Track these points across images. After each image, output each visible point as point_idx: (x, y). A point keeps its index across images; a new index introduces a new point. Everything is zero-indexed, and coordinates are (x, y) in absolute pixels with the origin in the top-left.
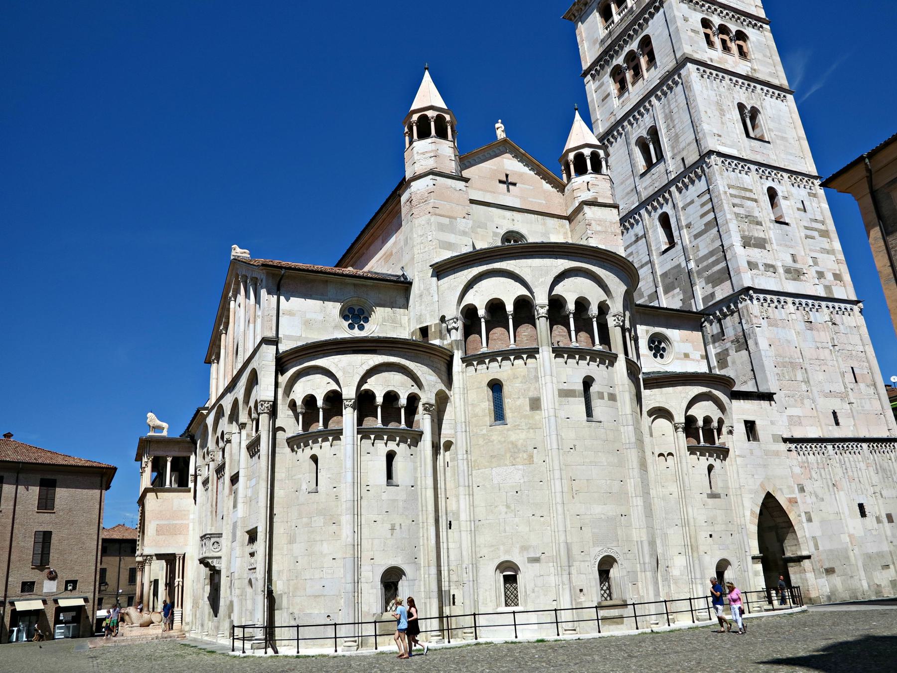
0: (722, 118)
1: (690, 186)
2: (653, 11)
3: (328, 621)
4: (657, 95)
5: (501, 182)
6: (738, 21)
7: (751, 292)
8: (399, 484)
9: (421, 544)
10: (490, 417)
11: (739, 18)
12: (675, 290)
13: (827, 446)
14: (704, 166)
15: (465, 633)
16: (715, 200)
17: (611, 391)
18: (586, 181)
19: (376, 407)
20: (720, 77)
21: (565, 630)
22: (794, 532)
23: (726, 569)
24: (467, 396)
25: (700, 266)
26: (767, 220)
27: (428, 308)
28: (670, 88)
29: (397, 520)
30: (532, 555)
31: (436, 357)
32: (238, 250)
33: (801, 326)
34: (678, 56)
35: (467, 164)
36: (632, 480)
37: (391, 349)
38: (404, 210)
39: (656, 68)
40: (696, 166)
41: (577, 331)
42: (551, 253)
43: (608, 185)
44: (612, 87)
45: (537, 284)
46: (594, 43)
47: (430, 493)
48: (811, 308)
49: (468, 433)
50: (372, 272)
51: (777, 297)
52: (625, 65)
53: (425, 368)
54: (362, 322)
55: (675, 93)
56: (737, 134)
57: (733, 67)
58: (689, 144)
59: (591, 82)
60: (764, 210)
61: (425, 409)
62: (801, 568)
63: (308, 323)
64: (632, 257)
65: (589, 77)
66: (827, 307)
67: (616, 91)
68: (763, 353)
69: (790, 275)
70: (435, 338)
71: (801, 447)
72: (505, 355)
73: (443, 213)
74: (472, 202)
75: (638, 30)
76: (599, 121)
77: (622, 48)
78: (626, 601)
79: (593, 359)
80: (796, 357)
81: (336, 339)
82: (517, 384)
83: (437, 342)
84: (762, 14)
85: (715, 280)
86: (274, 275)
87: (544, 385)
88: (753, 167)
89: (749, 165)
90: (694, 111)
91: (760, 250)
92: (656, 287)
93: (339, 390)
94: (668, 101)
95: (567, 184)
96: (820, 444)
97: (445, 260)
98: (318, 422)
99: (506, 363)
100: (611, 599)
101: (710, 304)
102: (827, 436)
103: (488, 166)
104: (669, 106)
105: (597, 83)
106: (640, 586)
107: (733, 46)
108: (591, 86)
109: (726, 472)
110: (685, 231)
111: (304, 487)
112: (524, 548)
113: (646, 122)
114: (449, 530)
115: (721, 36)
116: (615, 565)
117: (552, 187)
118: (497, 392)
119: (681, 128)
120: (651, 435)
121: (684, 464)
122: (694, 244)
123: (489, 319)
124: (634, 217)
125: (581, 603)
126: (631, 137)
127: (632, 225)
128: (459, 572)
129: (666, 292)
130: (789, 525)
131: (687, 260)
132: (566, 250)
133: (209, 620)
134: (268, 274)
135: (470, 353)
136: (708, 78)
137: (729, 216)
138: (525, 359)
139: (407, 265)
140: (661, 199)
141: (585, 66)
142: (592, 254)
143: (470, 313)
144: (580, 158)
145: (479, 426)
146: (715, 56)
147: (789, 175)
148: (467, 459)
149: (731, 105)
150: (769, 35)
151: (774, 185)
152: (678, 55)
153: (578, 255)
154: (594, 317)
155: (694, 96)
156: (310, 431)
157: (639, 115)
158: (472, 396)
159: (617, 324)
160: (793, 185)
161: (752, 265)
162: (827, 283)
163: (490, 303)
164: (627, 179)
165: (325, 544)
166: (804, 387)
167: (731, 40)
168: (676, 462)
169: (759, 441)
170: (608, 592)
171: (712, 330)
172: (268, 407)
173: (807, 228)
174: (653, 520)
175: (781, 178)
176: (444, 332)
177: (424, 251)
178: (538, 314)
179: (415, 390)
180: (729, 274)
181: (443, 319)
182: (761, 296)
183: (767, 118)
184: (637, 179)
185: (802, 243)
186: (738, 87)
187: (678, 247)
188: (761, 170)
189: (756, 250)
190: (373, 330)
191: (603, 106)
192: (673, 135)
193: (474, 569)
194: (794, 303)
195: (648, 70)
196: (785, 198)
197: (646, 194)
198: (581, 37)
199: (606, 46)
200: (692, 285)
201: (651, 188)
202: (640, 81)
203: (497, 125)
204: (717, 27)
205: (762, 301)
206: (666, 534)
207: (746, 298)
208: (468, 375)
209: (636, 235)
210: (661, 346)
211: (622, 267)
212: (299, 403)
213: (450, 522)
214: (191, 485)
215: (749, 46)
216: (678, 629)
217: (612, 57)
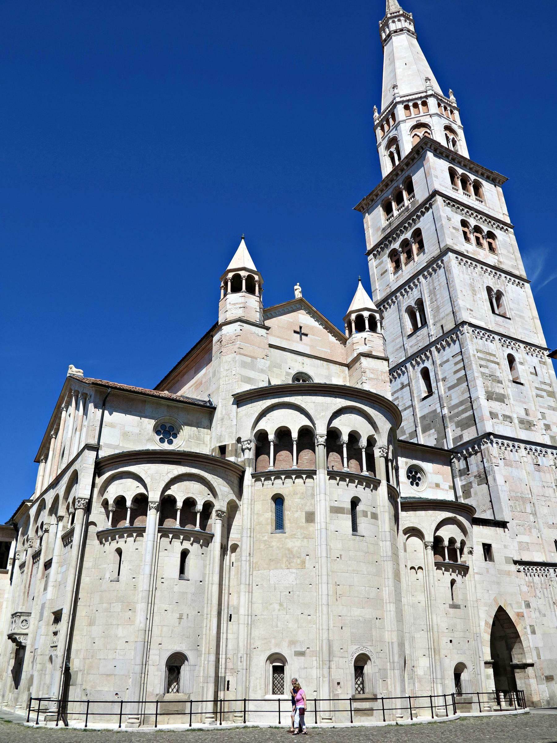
0: (474, 297)
1: (447, 348)
2: (424, 211)
3: (116, 699)
4: (424, 274)
5: (295, 332)
6: (489, 224)
7: (492, 437)
8: (190, 578)
9: (204, 633)
10: (272, 525)
11: (490, 222)
12: (431, 431)
13: (550, 570)
14: (458, 333)
15: (235, 717)
16: (466, 361)
17: (374, 510)
18: (364, 337)
19: (177, 510)
20: (474, 265)
21: (323, 719)
22: (521, 642)
23: (463, 672)
24: (254, 507)
25: (452, 412)
26: (506, 379)
27: (227, 430)
28: (435, 271)
29: (185, 611)
30: (299, 649)
31: (231, 471)
32: (74, 369)
33: (531, 468)
34: (442, 246)
35: (269, 316)
36: (387, 588)
37: (193, 462)
38: (215, 348)
39: (424, 253)
40: (452, 333)
41: (349, 459)
42: (331, 393)
43: (381, 341)
45: (318, 417)
46: (378, 230)
47: (216, 588)
48: (539, 454)
49: (252, 539)
50: (184, 396)
51: (513, 442)
52: (400, 249)
53: (220, 480)
54: (171, 438)
56: (485, 310)
57: (484, 258)
58: (447, 315)
59: (373, 260)
60: (504, 372)
61: (218, 515)
62: (526, 675)
63: (125, 435)
64: (398, 401)
65: (371, 256)
66: (552, 453)
67: (392, 269)
68: (500, 488)
69: (523, 425)
70: (231, 456)
71: (528, 569)
72: (288, 474)
73: (247, 353)
74: (271, 346)
75: (412, 224)
76: (378, 291)
77: (398, 236)
78: (376, 695)
79: (360, 483)
80: (526, 493)
81: (148, 450)
82: (297, 500)
83: (232, 459)
84: (508, 220)
85: (464, 425)
86: (101, 393)
87: (318, 502)
88: (497, 337)
89: (493, 335)
91: (500, 403)
92: (416, 427)
93: (146, 493)
94: (432, 280)
95: (349, 338)
96: (544, 568)
97: (243, 392)
98: (126, 519)
99: (288, 481)
100: (364, 693)
101: (459, 444)
102: (549, 560)
103: (286, 319)
104: (433, 284)
105: (378, 261)
106: (389, 683)
107: (485, 243)
108: (373, 263)
109: (466, 587)
110: (441, 384)
111: (108, 575)
112: (292, 643)
113: (414, 295)
114: (229, 623)
115: (475, 234)
116: (369, 662)
117: (336, 340)
118: (279, 505)
119: (442, 302)
120: (405, 551)
121: (431, 577)
122: (448, 394)
123: (277, 443)
124: (401, 369)
125: (338, 695)
126: (402, 306)
127: (399, 375)
128: (235, 660)
129: (424, 431)
130: (517, 636)
131: (442, 407)
132: (344, 392)
133: (10, 692)
134: (96, 391)
135: (259, 470)
136: (465, 265)
137: (476, 374)
138: (304, 478)
139: (213, 393)
140: (423, 356)
141: (369, 247)
142: (364, 396)
143: (262, 436)
144: (360, 319)
145: (261, 533)
146: (470, 248)
147: (525, 345)
148: (250, 561)
149: (481, 287)
150: (513, 237)
151: (513, 353)
152: (442, 246)
153: (354, 396)
154: (363, 448)
155: (453, 278)
156: (118, 527)
157: (409, 288)
158: (258, 507)
159: (382, 455)
160: (527, 354)
161: (493, 415)
162: (553, 435)
163: (279, 430)
164: (397, 339)
165: (120, 628)
166: (532, 518)
167: (483, 238)
168: (425, 575)
169: (494, 562)
170: (361, 686)
171: (459, 466)
172: (84, 504)
173: (537, 388)
174: (403, 624)
175: (519, 347)
176: (239, 451)
177: (228, 382)
178: (318, 442)
179: (211, 498)
180: (475, 421)
181: (239, 440)
182: (500, 441)
183: (509, 299)
184: (405, 339)
185: (534, 400)
186: (487, 274)
187: (435, 396)
188: (503, 340)
189: (497, 403)
190: (180, 444)
191: (381, 279)
192: (435, 307)
193: (248, 658)
194: (525, 448)
195: (418, 255)
196: (521, 363)
197: (411, 351)
198: (368, 225)
199: (387, 233)
200: (444, 427)
201: (416, 347)
202: (412, 262)
203: (296, 287)
204: (473, 227)
205: (500, 445)
206: (413, 638)
207: (488, 441)
208: (256, 489)
209: (402, 384)
210: (417, 476)
211: (389, 408)
212: (111, 502)
213: (231, 615)
214: (9, 567)
215: (497, 243)
216: (419, 723)
217: (390, 242)
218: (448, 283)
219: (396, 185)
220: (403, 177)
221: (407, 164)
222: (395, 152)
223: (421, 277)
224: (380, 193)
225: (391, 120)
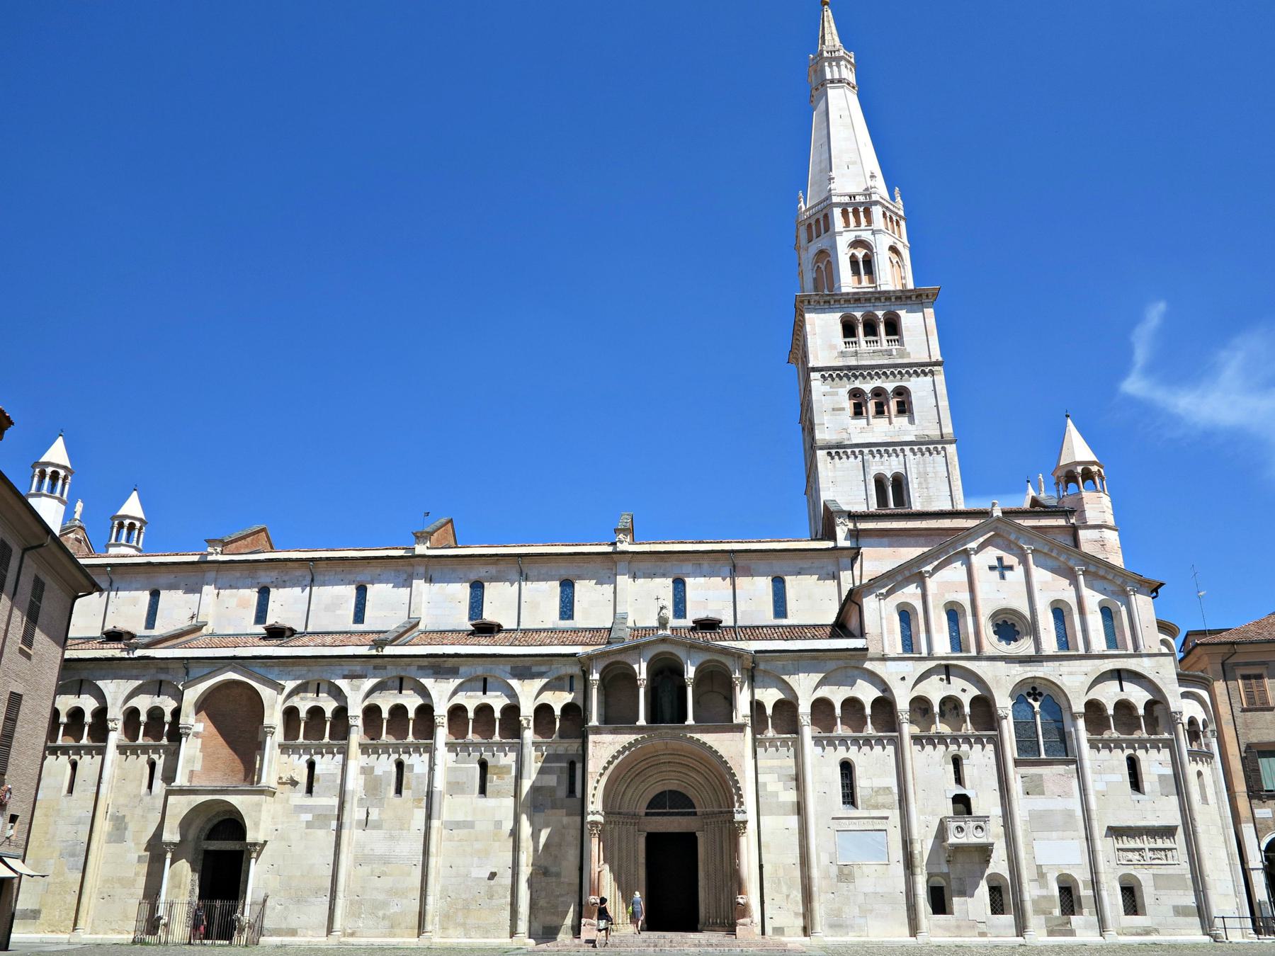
44: (848, 405)
52: (870, 395)
55: (933, 460)
76: (826, 426)
90: (955, 488)
94: (924, 461)
104: (925, 467)
105: (826, 388)
192: (925, 495)
198: (813, 329)
217: (856, 377)
218: (951, 479)
221: (898, 298)
222: (861, 260)
223: (907, 449)
224: (842, 302)
225: (862, 214)
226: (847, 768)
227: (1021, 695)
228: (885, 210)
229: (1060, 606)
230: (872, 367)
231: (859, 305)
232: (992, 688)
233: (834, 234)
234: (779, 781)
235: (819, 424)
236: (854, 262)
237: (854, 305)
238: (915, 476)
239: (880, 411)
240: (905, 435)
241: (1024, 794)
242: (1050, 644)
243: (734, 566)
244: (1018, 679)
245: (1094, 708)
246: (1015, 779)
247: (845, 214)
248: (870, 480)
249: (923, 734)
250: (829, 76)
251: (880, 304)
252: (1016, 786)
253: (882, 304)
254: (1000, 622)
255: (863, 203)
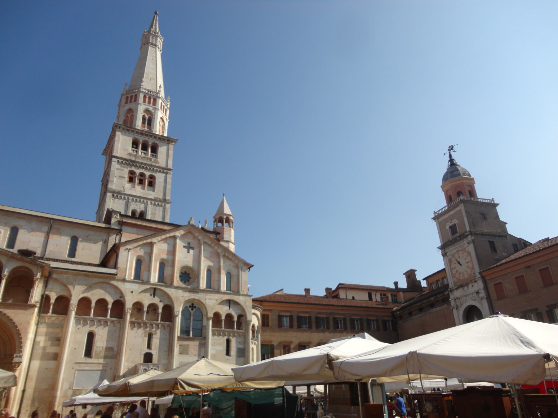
55: (159, 209)
59: (116, 163)
65: (116, 160)
76: (114, 183)
105: (118, 166)
217: (133, 165)
219: (147, 139)
220: (153, 141)
221: (160, 139)
223: (149, 202)
225: (152, 100)
226: (91, 336)
227: (187, 307)
228: (162, 101)
229: (211, 269)
230: (142, 163)
231: (142, 136)
232: (174, 301)
233: (138, 104)
234: (48, 341)
235: (111, 181)
236: (144, 118)
237: (140, 136)
238: (150, 214)
239: (141, 182)
240: (150, 195)
241: (179, 354)
242: (203, 284)
243: (51, 227)
244: (187, 299)
245: (217, 316)
246: (177, 346)
247: (145, 97)
248: (129, 211)
249: (136, 321)
250: (151, 41)
251: (151, 138)
252: (176, 350)
253: (152, 139)
254: (183, 272)
255: (154, 96)
